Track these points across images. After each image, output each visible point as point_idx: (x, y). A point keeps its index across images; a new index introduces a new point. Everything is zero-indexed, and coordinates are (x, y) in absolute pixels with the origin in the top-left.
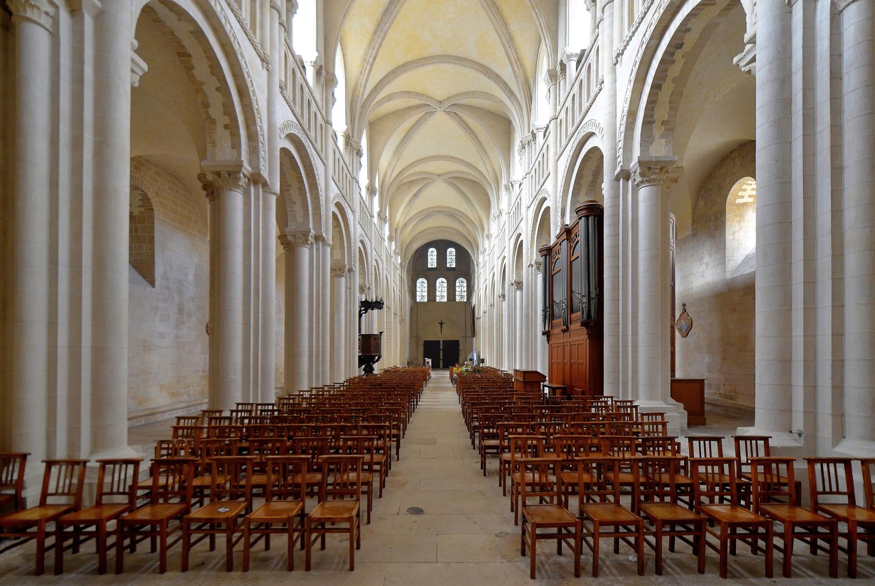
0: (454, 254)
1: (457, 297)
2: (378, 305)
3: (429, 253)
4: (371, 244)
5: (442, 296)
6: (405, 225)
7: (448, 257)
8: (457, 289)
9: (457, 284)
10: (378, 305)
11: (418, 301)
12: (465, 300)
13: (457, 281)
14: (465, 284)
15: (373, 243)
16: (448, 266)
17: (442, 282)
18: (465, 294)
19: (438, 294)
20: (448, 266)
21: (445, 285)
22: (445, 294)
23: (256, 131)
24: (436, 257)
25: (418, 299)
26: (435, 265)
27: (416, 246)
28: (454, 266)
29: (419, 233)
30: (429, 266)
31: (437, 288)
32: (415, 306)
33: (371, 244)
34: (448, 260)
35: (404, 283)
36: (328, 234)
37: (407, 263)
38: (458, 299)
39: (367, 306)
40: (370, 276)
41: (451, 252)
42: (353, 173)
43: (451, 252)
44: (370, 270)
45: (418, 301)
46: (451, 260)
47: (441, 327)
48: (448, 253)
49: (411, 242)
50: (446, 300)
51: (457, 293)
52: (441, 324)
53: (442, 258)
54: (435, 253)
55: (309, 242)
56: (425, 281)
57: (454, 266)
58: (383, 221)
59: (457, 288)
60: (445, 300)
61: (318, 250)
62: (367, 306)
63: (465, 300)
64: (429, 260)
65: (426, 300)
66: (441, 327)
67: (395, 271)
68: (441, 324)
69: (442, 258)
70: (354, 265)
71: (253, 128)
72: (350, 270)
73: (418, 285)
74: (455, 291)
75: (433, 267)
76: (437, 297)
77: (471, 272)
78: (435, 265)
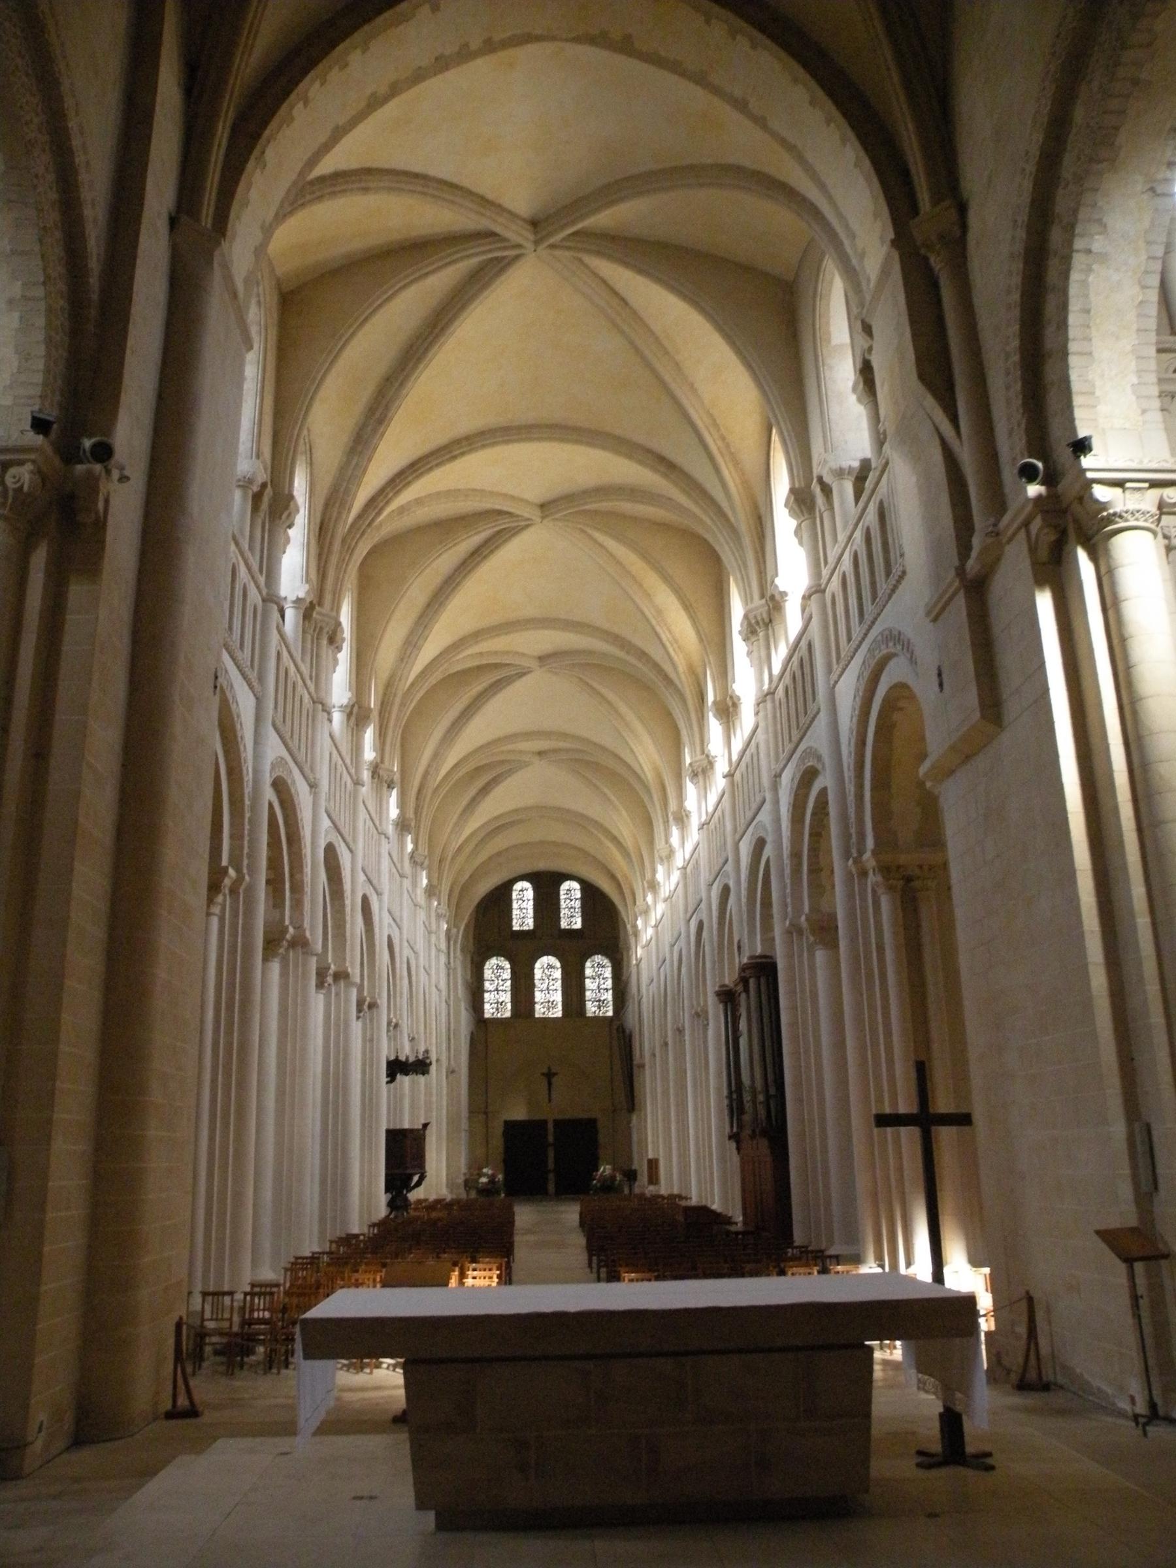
0: (579, 895)
1: (589, 1005)
2: (420, 1066)
3: (514, 895)
4: (401, 933)
5: (551, 1004)
6: (460, 849)
7: (563, 904)
8: (588, 983)
9: (588, 972)
10: (420, 1066)
11: (487, 1015)
12: (610, 1014)
13: (588, 964)
14: (608, 972)
15: (405, 931)
16: (564, 924)
17: (550, 966)
18: (609, 996)
19: (539, 996)
20: (564, 924)
21: (558, 974)
22: (558, 997)
23: (302, 881)
24: (531, 903)
25: (489, 1011)
26: (529, 924)
27: (484, 887)
28: (578, 924)
29: (490, 858)
30: (516, 928)
31: (537, 982)
32: (482, 1025)
33: (401, 933)
34: (563, 912)
35: (455, 978)
36: (355, 973)
37: (462, 928)
38: (591, 1009)
39: (396, 1068)
40: (398, 999)
41: (570, 894)
42: (380, 824)
43: (570, 894)
44: (398, 988)
45: (487, 1015)
46: (571, 917)
47: (550, 1084)
48: (562, 893)
49: (473, 879)
50: (559, 1014)
51: (588, 994)
52: (549, 1076)
53: (547, 904)
54: (530, 894)
55: (326, 985)
56: (507, 965)
57: (578, 924)
58: (419, 868)
59: (587, 981)
60: (558, 1013)
61: (337, 994)
62: (396, 1068)
63: (610, 1014)
64: (515, 912)
65: (508, 1014)
66: (550, 1084)
67: (437, 957)
68: (549, 1076)
69: (547, 904)
70: (379, 994)
71: (298, 876)
72: (372, 1006)
73: (488, 974)
74: (582, 989)
75: (526, 928)
76: (537, 1007)
77: (621, 944)
78: (529, 924)
